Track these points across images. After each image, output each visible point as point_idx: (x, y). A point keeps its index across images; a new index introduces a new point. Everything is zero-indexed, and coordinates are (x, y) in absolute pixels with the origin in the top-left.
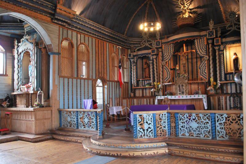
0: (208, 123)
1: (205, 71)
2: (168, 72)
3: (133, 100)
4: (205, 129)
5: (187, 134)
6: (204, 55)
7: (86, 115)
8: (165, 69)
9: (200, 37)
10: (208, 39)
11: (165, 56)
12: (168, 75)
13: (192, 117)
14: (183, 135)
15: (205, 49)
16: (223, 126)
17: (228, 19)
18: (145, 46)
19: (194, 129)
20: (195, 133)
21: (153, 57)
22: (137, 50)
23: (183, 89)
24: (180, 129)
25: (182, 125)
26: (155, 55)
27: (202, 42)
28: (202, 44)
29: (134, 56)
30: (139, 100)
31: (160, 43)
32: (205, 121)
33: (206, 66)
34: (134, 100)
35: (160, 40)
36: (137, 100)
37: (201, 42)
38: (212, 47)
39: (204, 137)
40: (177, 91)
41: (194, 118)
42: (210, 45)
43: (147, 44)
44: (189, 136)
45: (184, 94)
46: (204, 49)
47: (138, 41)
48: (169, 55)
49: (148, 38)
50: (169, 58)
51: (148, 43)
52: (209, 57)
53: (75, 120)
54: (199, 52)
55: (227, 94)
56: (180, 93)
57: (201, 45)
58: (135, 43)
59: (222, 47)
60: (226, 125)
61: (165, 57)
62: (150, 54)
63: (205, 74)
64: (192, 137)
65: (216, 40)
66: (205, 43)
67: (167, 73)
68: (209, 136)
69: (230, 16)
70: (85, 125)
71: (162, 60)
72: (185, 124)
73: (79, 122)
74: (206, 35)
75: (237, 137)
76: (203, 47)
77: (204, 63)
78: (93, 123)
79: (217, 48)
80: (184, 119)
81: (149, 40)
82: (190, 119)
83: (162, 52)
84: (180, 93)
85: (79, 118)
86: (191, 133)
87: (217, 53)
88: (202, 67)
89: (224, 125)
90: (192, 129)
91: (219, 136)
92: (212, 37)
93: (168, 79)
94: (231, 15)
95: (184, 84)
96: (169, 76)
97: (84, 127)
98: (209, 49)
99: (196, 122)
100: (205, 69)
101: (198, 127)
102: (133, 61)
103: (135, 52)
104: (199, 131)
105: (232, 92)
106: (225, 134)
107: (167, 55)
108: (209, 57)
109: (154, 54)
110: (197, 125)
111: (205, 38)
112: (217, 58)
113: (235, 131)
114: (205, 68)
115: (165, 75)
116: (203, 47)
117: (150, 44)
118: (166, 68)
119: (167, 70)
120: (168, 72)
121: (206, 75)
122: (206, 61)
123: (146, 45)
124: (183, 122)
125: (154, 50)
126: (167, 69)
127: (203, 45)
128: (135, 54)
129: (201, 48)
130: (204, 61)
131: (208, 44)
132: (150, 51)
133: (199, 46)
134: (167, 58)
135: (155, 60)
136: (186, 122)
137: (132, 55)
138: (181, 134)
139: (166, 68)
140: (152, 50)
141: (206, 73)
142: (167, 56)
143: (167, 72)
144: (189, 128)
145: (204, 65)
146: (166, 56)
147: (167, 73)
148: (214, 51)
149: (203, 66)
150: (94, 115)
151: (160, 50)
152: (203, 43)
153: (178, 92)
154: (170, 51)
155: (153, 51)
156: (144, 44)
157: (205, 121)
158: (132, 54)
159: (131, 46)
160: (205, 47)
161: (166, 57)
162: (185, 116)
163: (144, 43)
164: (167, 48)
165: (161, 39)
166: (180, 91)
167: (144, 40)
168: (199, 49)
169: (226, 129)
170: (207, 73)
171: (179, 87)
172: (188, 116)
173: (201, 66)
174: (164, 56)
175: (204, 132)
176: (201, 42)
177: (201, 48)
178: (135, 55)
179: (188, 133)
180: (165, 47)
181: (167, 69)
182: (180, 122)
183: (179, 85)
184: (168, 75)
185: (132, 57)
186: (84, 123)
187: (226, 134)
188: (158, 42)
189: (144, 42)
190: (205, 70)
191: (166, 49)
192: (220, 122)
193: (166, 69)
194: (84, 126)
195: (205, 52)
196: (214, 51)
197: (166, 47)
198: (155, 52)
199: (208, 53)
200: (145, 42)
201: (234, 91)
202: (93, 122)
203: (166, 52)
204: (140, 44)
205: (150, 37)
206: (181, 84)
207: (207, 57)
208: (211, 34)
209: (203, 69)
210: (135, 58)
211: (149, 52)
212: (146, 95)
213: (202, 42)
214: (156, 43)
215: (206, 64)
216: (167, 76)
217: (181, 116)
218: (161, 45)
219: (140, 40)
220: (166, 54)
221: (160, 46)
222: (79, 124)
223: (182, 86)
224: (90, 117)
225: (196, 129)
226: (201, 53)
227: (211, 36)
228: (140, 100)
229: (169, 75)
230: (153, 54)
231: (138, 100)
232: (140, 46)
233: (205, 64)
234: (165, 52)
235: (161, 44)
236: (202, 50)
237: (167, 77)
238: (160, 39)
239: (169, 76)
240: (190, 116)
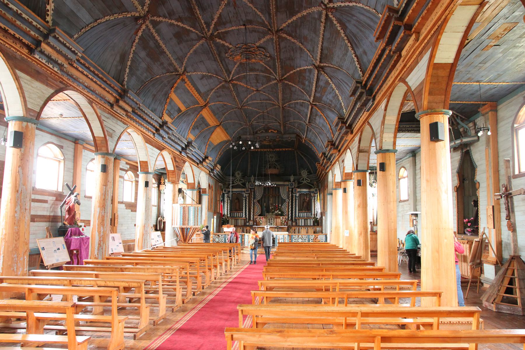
9: (284, 185)
10: (289, 188)
42: (290, 193)
43: (240, 183)
53: (223, 240)
55: (299, 226)
62: (244, 192)
71: (254, 198)
74: (288, 185)
79: (294, 195)
83: (254, 192)
132: (243, 190)
135: (247, 198)
148: (292, 196)
151: (253, 190)
155: (247, 191)
196: (292, 196)
201: (303, 224)
208: (292, 185)
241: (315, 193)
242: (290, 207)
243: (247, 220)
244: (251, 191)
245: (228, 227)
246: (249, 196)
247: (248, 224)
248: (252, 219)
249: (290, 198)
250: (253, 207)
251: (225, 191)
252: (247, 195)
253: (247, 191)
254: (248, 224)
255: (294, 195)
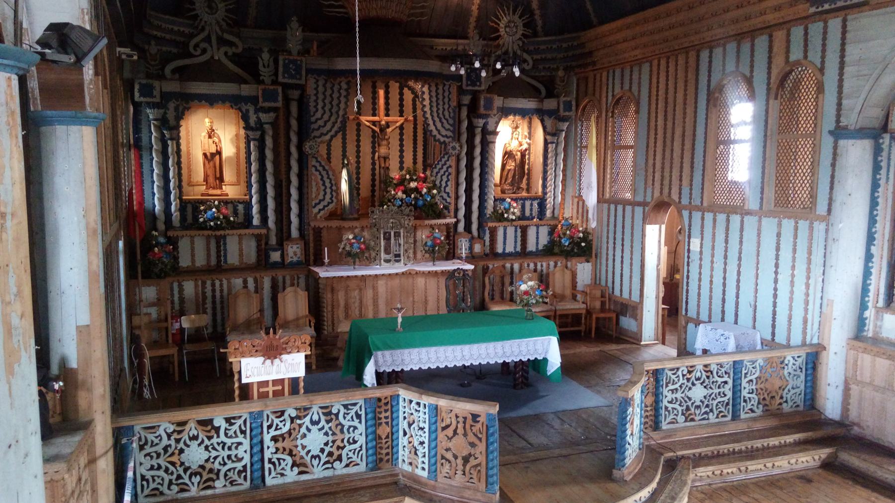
0: (726, 382)
1: (448, 190)
2: (327, 181)
3: (175, 285)
4: (719, 399)
5: (681, 419)
6: (446, 139)
7: (315, 418)
8: (317, 170)
10: (461, 92)
11: (317, 120)
12: (324, 190)
13: (693, 374)
14: (673, 423)
15: (451, 122)
16: (754, 387)
17: (500, 36)
18: (207, 63)
19: (698, 403)
20: (698, 412)
21: (261, 115)
22: (174, 71)
23: (400, 245)
24: (666, 408)
25: (670, 396)
26: (275, 110)
27: (444, 97)
28: (444, 104)
29: (166, 97)
30: (209, 283)
31: (301, 66)
32: (720, 380)
33: (450, 174)
34: (184, 283)
35: (304, 59)
36: (196, 286)
37: (441, 97)
38: (468, 117)
39: (717, 417)
40: (379, 251)
41: (699, 374)
42: (464, 112)
43: (219, 55)
44: (686, 421)
45: (400, 261)
46: (447, 120)
47: (180, 33)
48: (333, 119)
49: (222, 31)
50: (332, 133)
51: (223, 49)
52: (461, 147)
53: (244, 452)
54: (432, 127)
56: (388, 257)
57: (441, 107)
58: (168, 36)
59: (491, 121)
60: (759, 382)
61: (313, 126)
63: (445, 196)
64: (692, 423)
65: (485, 98)
66: (454, 104)
67: (324, 184)
68: (726, 413)
69: (508, 30)
70: (308, 459)
72: (679, 395)
73: (267, 454)
75: (776, 407)
76: (446, 113)
77: (445, 164)
78: (353, 447)
80: (676, 380)
81: (227, 36)
82: (688, 380)
83: (302, 103)
84: (388, 257)
85: (267, 438)
86: (691, 414)
87: (478, 140)
88: (439, 175)
89: (757, 384)
90: (693, 404)
91: (746, 409)
92: (476, 88)
93: (325, 207)
94: (509, 26)
95: (402, 231)
96: (328, 196)
97: (300, 473)
98: (460, 122)
99: (701, 384)
100: (446, 182)
101: (705, 397)
102: (160, 117)
103: (161, 77)
104: (707, 406)
105: (507, 251)
106: (756, 404)
107: (326, 117)
108: (461, 147)
109: (272, 104)
110: (705, 392)
111: (454, 90)
112: (478, 151)
113: (774, 394)
114: (448, 180)
115: (314, 190)
116: (446, 113)
117: (230, 53)
118: (321, 165)
119: (324, 173)
120: (327, 181)
121: (448, 200)
122: (454, 158)
123: (212, 57)
124: (672, 390)
125: (276, 91)
126: (324, 169)
127: (446, 106)
128: (172, 86)
129: (441, 116)
130: (446, 157)
131: (460, 106)
133: (435, 109)
134: (324, 130)
135: (270, 132)
136: (681, 386)
137: (156, 93)
138: (668, 420)
139: (317, 165)
140: (264, 90)
141: (448, 193)
142: (326, 122)
143: (322, 179)
144: (686, 402)
145: (445, 168)
146: (321, 123)
147: (324, 184)
148: (471, 129)
149: (442, 172)
150: (363, 413)
151: (295, 94)
152: (446, 100)
153: (383, 256)
154: (338, 105)
156: (204, 51)
157: (720, 380)
158: (156, 84)
159: (147, 47)
160: (452, 115)
161: (320, 126)
162: (680, 373)
163: (203, 45)
164: (324, 94)
165: (305, 52)
166: (387, 251)
167: (206, 33)
168: (432, 116)
169: (760, 391)
170: (453, 195)
171: (387, 239)
172: (685, 373)
173: (437, 173)
174: (313, 119)
175: (717, 405)
176: (441, 97)
177: (441, 116)
178: (167, 93)
179: (683, 414)
180: (316, 89)
181: (324, 169)
182: (665, 392)
183: (385, 233)
184: (324, 190)
185: (157, 100)
186: (303, 453)
187: (759, 403)
188: (294, 62)
189: (203, 40)
190: (447, 185)
191: (321, 96)
192: (749, 378)
193: (320, 169)
194: (305, 465)
195: (452, 129)
196: (471, 129)
197: (321, 89)
198: (276, 100)
199: (457, 137)
200: (208, 39)
202: (355, 442)
203: (319, 107)
204: (185, 45)
205: (228, 24)
206: (392, 228)
207: (457, 145)
209: (442, 180)
210: (172, 105)
211: (243, 93)
212: (226, 261)
213: (444, 97)
214: (286, 66)
215: (450, 166)
216: (322, 193)
217: (670, 373)
218: (304, 78)
219: (187, 31)
220: (318, 115)
221: (302, 82)
222: (267, 465)
223: (397, 235)
224: (340, 424)
225: (701, 401)
226: (439, 131)
227: (474, 84)
228: (213, 285)
229: (328, 191)
230: (267, 104)
231: (204, 283)
232: (175, 50)
233: (448, 168)
234: (315, 107)
235: (304, 73)
236: (442, 123)
237: (321, 197)
238: (299, 53)
239: (328, 196)
240: (690, 372)
241: (563, 119)
242: (463, 175)
243: (273, 241)
244: (287, 100)
245: (272, 352)
246: (274, 125)
247: (275, 256)
248: (295, 233)
249: (464, 137)
250: (300, 176)
251: (147, 91)
252: (264, 117)
253: (270, 96)
254: (275, 256)
255: (481, 122)
